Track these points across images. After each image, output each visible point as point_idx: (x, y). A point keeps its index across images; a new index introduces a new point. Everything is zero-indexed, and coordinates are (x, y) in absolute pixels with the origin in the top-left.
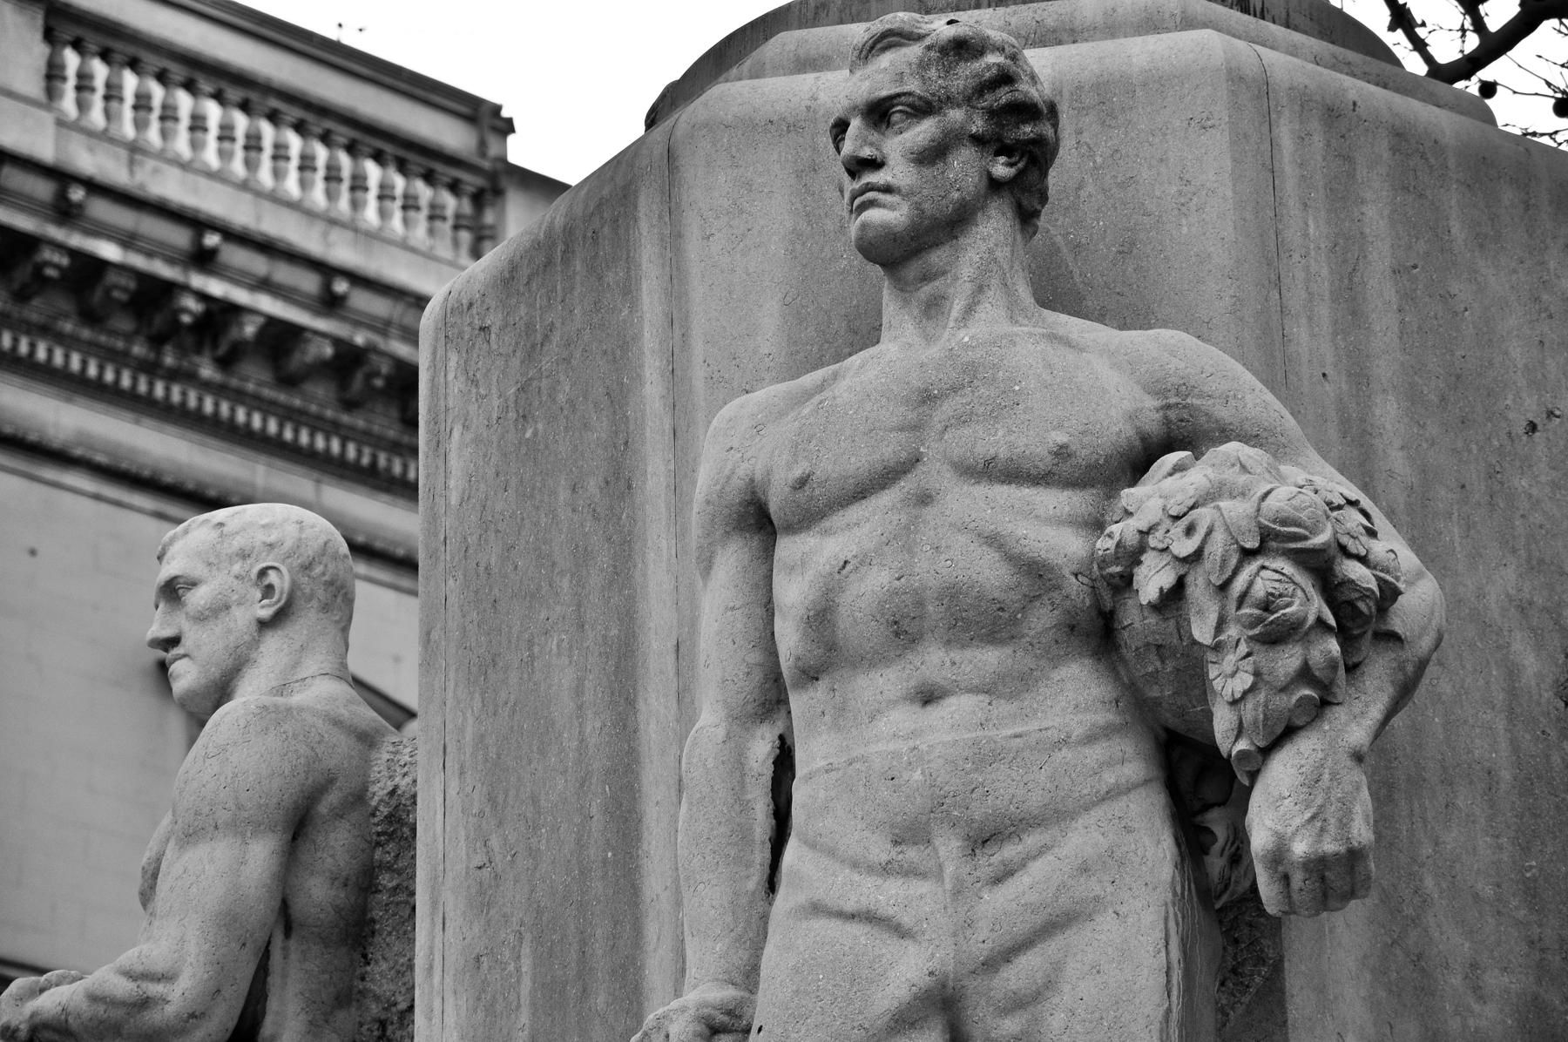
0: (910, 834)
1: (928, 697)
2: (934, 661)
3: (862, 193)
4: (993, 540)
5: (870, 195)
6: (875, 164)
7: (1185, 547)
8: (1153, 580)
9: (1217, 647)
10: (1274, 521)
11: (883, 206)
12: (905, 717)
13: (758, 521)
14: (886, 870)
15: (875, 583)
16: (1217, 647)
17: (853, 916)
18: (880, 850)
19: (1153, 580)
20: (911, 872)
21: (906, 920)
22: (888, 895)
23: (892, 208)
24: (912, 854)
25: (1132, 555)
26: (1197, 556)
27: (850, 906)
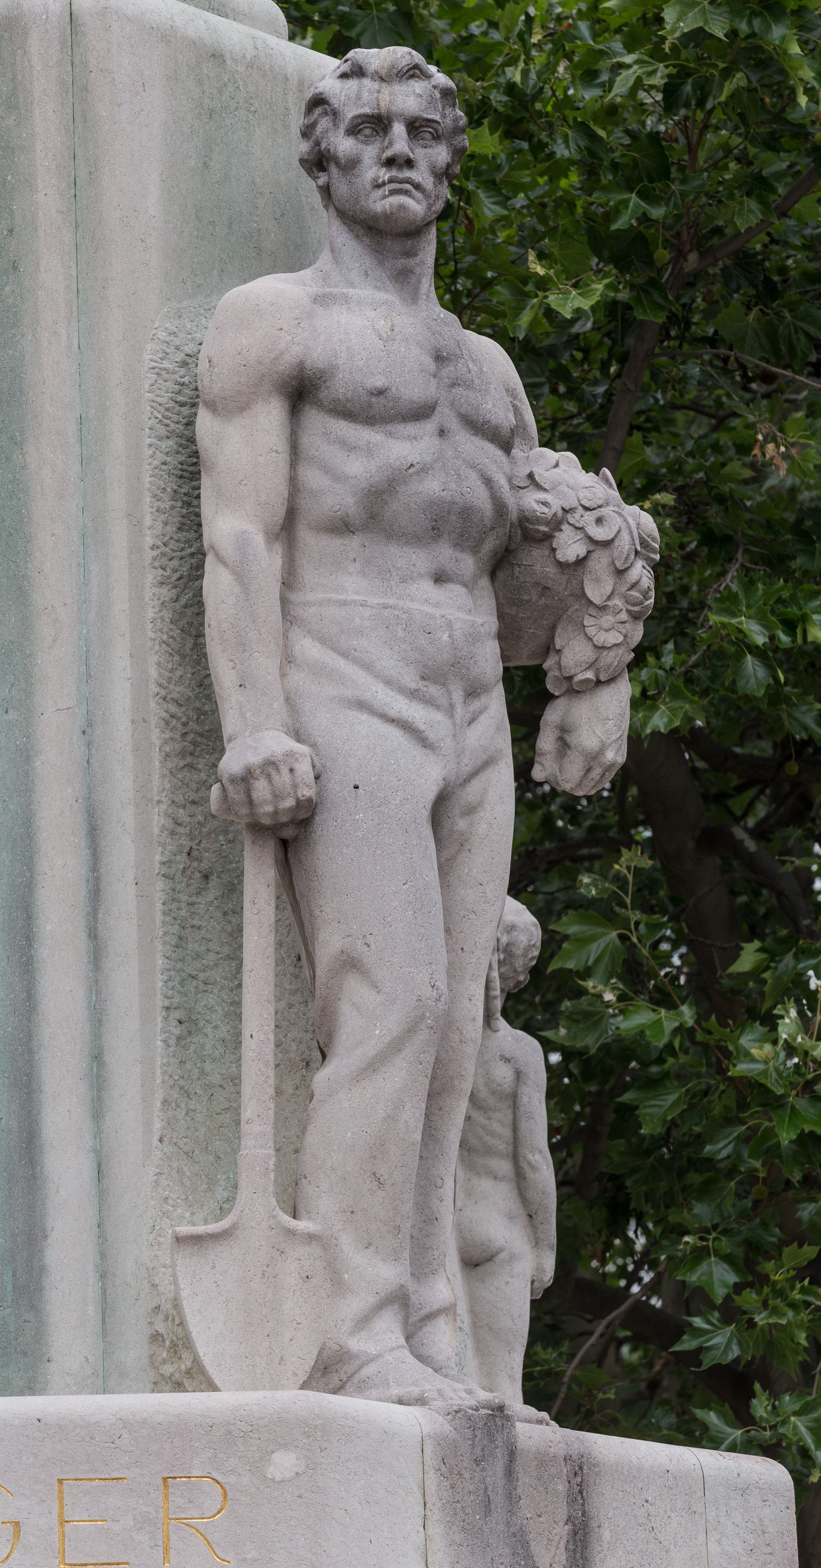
0: (433, 674)
1: (440, 578)
2: (445, 553)
3: (402, 182)
4: (488, 482)
5: (408, 187)
6: (409, 163)
7: (600, 533)
8: (570, 547)
9: (602, 609)
10: (649, 536)
11: (414, 198)
12: (426, 587)
13: (301, 391)
14: (413, 695)
15: (432, 486)
16: (602, 609)
17: (393, 721)
18: (411, 680)
19: (570, 547)
20: (429, 702)
21: (431, 735)
22: (417, 713)
23: (418, 202)
24: (433, 690)
25: (556, 523)
26: (607, 544)
27: (392, 713)
